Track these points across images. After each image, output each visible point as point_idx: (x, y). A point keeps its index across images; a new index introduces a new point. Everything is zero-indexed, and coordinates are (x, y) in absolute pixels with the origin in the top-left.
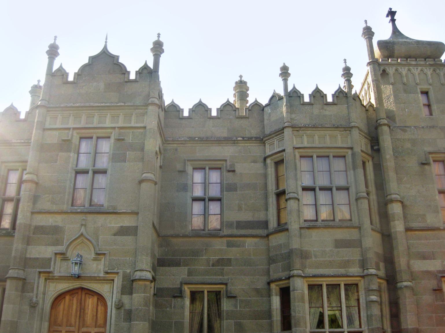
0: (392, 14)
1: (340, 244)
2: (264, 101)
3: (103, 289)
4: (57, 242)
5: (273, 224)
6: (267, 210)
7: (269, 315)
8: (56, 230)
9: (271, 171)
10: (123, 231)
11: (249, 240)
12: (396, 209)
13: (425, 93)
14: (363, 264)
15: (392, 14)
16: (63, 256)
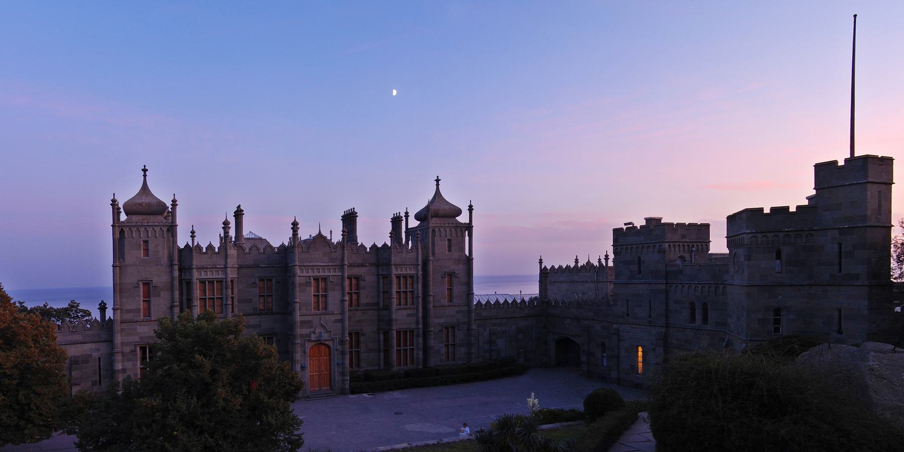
0: (438, 181)
1: (409, 315)
2: (380, 246)
3: (330, 343)
4: (311, 327)
5: (381, 305)
6: (378, 297)
7: (379, 342)
8: (309, 322)
9: (381, 281)
10: (337, 321)
11: (370, 312)
12: (431, 299)
13: (449, 240)
14: (417, 323)
15: (438, 181)
16: (314, 333)
